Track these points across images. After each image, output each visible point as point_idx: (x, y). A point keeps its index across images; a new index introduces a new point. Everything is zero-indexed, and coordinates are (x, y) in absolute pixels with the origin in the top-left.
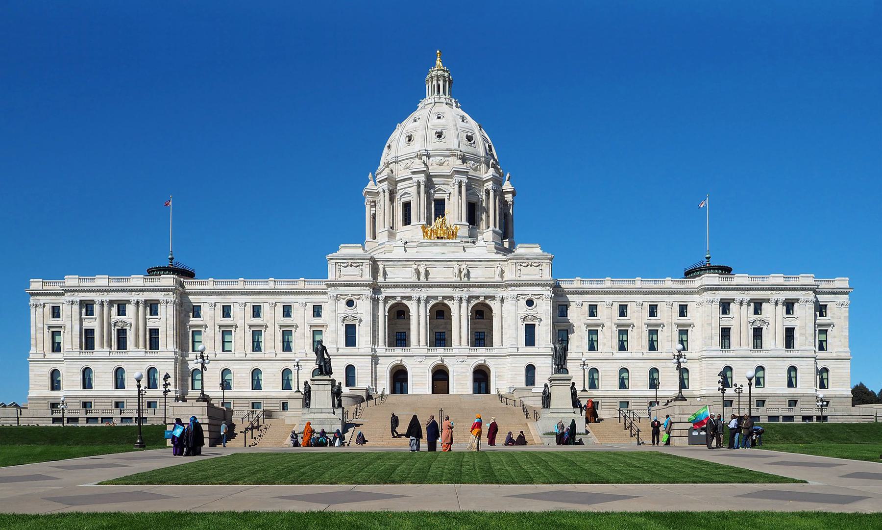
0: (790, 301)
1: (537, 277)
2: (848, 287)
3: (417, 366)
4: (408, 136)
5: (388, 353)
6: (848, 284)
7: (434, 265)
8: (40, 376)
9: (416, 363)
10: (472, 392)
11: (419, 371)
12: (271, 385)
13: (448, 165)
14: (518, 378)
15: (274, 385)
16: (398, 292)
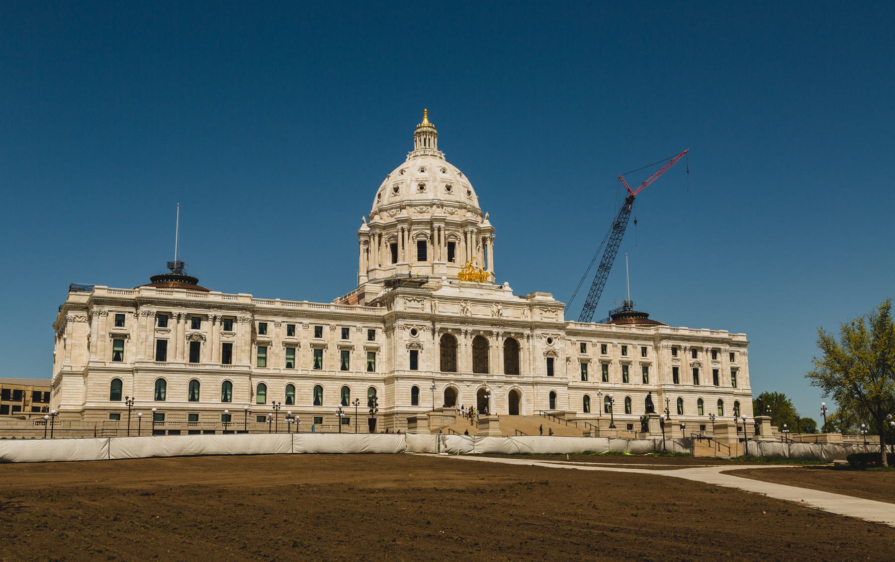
0: (695, 348)
1: (554, 321)
2: (746, 341)
3: (466, 389)
4: (421, 185)
5: (443, 377)
6: (746, 339)
7: (476, 304)
8: (100, 385)
9: (465, 387)
10: (508, 413)
11: (468, 394)
12: (332, 401)
13: (457, 215)
14: (544, 403)
15: (334, 401)
16: (450, 326)
